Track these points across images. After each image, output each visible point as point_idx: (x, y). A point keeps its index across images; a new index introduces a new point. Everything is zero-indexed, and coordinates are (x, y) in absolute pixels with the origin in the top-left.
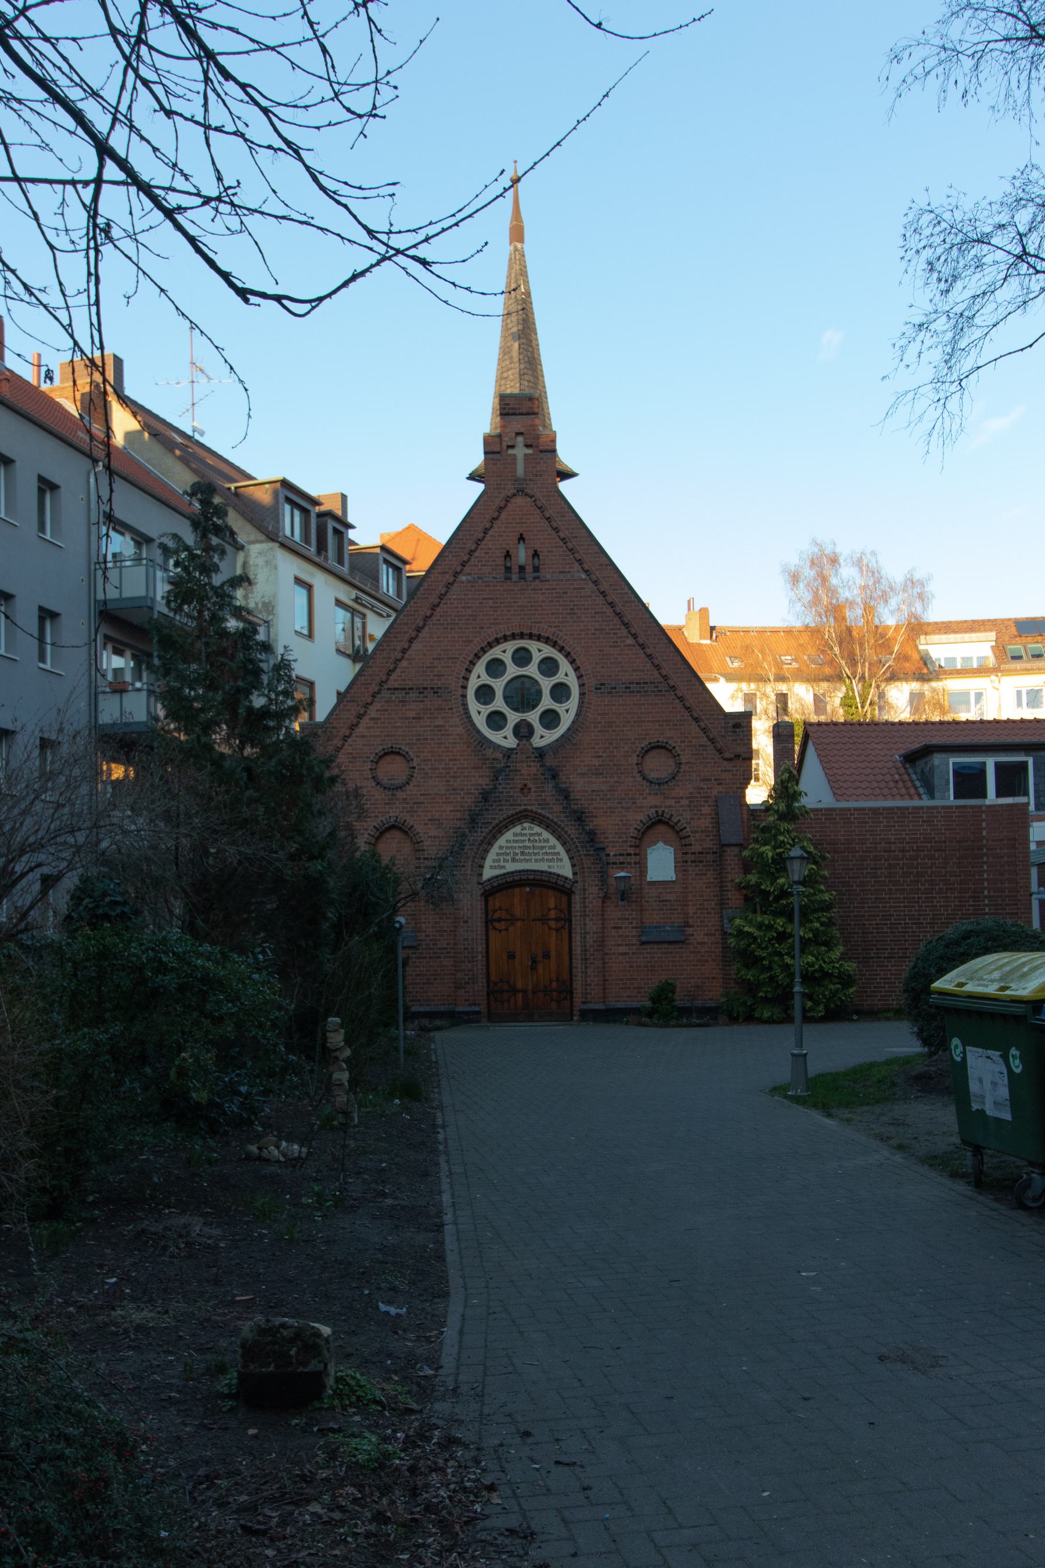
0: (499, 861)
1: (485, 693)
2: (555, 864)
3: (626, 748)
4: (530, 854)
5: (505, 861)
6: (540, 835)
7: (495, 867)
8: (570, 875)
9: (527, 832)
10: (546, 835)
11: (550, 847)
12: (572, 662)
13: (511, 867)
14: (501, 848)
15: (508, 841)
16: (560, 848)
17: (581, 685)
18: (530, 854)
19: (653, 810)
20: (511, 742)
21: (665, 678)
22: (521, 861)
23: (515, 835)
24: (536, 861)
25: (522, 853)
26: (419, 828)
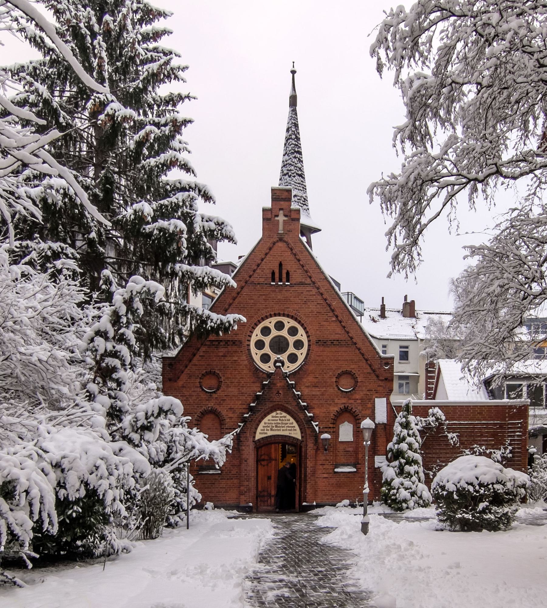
0: (264, 430)
1: (260, 345)
2: (292, 432)
3: (331, 374)
4: (280, 427)
5: (267, 430)
6: (285, 417)
7: (262, 433)
8: (300, 438)
9: (279, 415)
10: (288, 417)
11: (290, 424)
12: (305, 329)
13: (270, 433)
14: (265, 423)
15: (269, 420)
16: (295, 424)
17: (309, 341)
18: (280, 427)
19: (343, 405)
20: (272, 370)
21: (352, 338)
22: (275, 430)
23: (273, 417)
24: (283, 430)
25: (276, 426)
26: (224, 413)
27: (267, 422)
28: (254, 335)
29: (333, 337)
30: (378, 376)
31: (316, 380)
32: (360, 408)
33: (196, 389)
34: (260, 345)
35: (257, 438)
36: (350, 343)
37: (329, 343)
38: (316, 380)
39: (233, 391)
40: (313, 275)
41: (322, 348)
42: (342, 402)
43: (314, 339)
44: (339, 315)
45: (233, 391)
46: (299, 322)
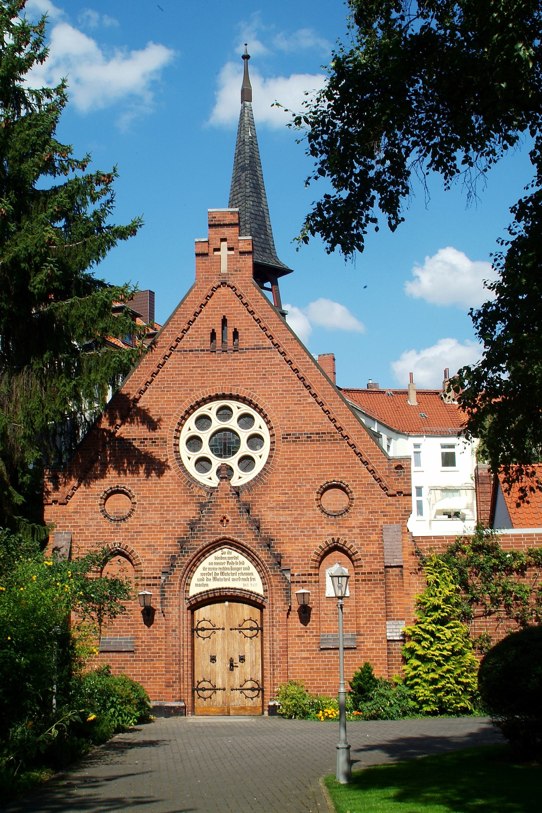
0: (202, 580)
1: (194, 442)
2: (249, 583)
3: (308, 486)
4: (228, 574)
5: (208, 580)
6: (237, 558)
7: (200, 585)
8: (261, 592)
9: (226, 556)
10: (242, 558)
11: (245, 569)
12: (265, 417)
13: (213, 585)
14: (204, 569)
15: (210, 564)
16: (253, 570)
17: (272, 436)
18: (228, 574)
19: (330, 538)
20: (215, 482)
21: (340, 429)
22: (221, 580)
23: (216, 558)
24: (234, 580)
25: (222, 574)
26: (138, 553)
27: (207, 566)
28: (184, 430)
29: (308, 429)
30: (385, 489)
31: (283, 498)
32: (358, 541)
33: (95, 516)
34: (194, 442)
35: (191, 594)
36: (338, 436)
37: (304, 438)
38: (283, 498)
39: (153, 518)
40: (275, 335)
41: (293, 446)
42: (327, 533)
43: (279, 433)
44: (319, 394)
45: (153, 518)
46: (255, 407)
